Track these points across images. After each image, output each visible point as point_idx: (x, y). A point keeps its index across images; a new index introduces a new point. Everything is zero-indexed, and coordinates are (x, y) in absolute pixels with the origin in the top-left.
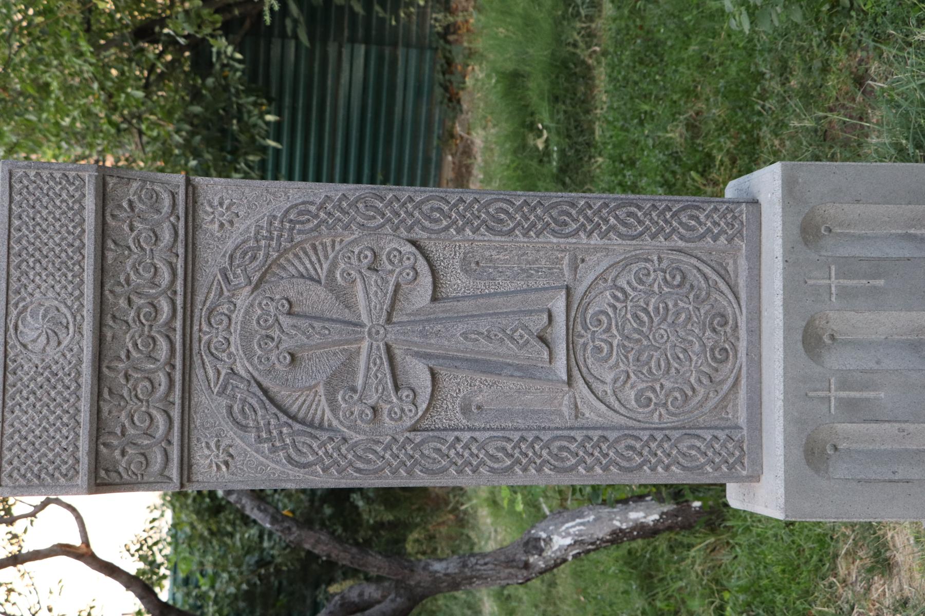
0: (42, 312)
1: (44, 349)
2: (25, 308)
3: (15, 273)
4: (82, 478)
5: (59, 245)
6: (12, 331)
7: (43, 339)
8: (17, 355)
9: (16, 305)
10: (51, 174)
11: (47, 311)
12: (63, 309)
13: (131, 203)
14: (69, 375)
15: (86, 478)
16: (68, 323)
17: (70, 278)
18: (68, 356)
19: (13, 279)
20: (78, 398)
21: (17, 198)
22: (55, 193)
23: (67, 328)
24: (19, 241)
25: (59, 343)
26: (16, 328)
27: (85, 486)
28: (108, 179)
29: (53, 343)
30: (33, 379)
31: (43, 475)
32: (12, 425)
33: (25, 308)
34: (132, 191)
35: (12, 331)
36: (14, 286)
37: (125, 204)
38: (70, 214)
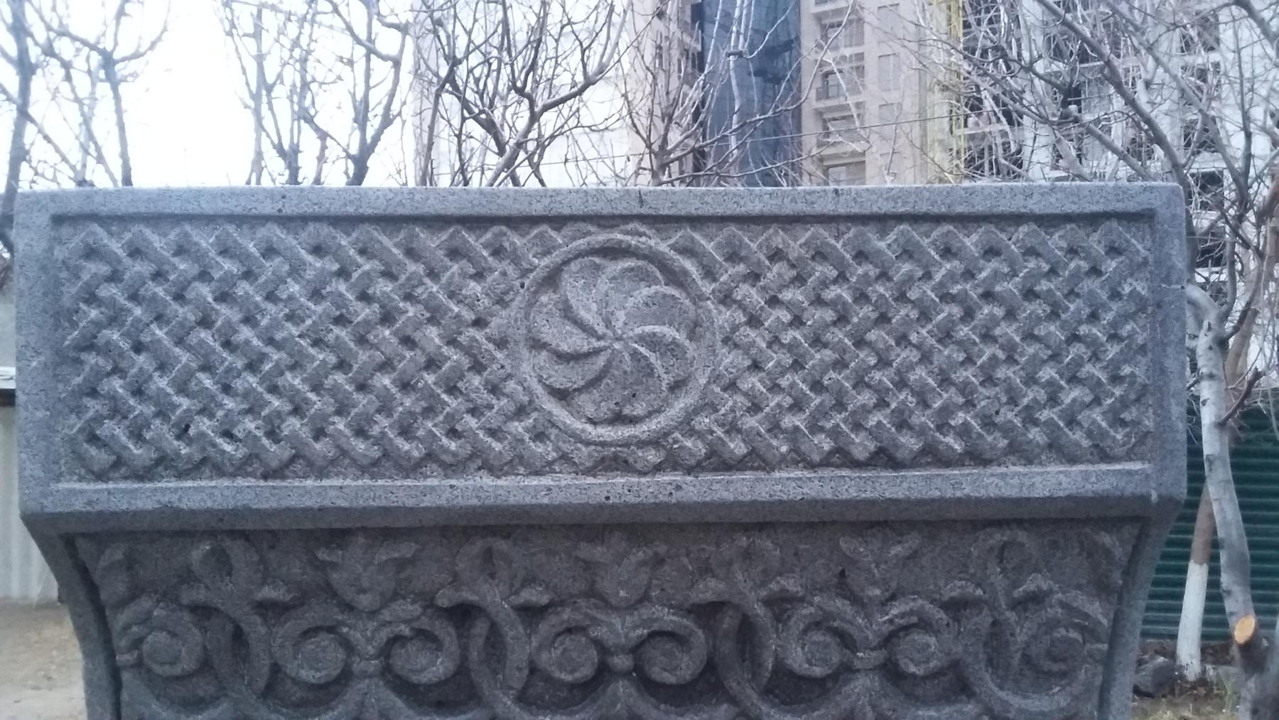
0: (668, 332)
1: (537, 345)
2: (676, 278)
3: (796, 243)
4: (79, 494)
5: (901, 384)
6: (601, 237)
7: (574, 341)
8: (516, 259)
9: (688, 251)
10: (1143, 349)
11: (670, 349)
12: (680, 405)
13: (1037, 598)
14: (453, 433)
15: (78, 505)
16: (633, 421)
17: (788, 421)
18: (517, 427)
19: (779, 238)
20: (370, 468)
21: (1057, 241)
22: (1078, 363)
23: (618, 419)
24: (907, 253)
25: (562, 395)
26: (612, 252)
27: (50, 506)
28: (1129, 531)
29: (562, 376)
30: (435, 315)
31: (91, 359)
32: (269, 251)
33: (676, 278)
34: (1082, 601)
35: (601, 237)
36: (753, 243)
37: (1035, 582)
38: (1008, 415)
